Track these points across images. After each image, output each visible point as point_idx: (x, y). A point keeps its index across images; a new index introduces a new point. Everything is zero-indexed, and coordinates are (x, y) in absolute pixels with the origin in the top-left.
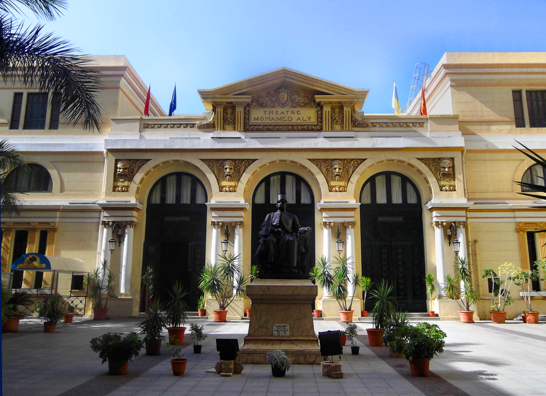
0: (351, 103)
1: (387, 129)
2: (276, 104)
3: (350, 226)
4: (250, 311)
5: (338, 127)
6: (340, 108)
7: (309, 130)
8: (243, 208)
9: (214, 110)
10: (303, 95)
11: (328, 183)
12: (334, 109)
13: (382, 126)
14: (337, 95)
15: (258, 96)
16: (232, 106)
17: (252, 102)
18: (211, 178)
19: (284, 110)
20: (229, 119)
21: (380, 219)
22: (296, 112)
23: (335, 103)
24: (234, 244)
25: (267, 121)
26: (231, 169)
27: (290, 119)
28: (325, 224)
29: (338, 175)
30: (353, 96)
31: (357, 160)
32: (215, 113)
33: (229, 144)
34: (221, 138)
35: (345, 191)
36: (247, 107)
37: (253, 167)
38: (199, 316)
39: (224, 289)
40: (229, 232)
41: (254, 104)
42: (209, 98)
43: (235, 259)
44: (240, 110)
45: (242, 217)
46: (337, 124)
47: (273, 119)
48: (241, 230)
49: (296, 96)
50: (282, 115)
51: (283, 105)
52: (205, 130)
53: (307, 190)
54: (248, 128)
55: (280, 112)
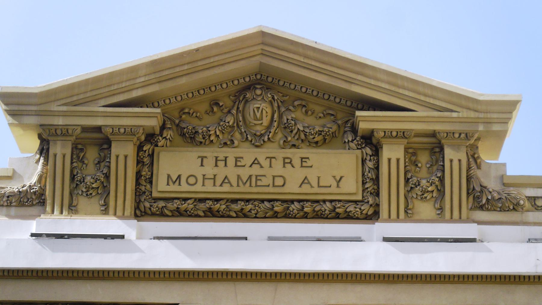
5: (426, 208)
6: (432, 152)
7: (336, 216)
9: (44, 150)
10: (318, 109)
12: (414, 154)
14: (422, 113)
15: (183, 109)
16: (101, 140)
17: (163, 127)
19: (261, 154)
20: (88, 179)
22: (297, 162)
23: (418, 135)
30: (472, 114)
32: (47, 160)
41: (168, 134)
42: (28, 114)
44: (123, 151)
49: (298, 114)
50: (256, 170)
51: (258, 140)
52: (13, 211)
54: (147, 207)
55: (248, 160)
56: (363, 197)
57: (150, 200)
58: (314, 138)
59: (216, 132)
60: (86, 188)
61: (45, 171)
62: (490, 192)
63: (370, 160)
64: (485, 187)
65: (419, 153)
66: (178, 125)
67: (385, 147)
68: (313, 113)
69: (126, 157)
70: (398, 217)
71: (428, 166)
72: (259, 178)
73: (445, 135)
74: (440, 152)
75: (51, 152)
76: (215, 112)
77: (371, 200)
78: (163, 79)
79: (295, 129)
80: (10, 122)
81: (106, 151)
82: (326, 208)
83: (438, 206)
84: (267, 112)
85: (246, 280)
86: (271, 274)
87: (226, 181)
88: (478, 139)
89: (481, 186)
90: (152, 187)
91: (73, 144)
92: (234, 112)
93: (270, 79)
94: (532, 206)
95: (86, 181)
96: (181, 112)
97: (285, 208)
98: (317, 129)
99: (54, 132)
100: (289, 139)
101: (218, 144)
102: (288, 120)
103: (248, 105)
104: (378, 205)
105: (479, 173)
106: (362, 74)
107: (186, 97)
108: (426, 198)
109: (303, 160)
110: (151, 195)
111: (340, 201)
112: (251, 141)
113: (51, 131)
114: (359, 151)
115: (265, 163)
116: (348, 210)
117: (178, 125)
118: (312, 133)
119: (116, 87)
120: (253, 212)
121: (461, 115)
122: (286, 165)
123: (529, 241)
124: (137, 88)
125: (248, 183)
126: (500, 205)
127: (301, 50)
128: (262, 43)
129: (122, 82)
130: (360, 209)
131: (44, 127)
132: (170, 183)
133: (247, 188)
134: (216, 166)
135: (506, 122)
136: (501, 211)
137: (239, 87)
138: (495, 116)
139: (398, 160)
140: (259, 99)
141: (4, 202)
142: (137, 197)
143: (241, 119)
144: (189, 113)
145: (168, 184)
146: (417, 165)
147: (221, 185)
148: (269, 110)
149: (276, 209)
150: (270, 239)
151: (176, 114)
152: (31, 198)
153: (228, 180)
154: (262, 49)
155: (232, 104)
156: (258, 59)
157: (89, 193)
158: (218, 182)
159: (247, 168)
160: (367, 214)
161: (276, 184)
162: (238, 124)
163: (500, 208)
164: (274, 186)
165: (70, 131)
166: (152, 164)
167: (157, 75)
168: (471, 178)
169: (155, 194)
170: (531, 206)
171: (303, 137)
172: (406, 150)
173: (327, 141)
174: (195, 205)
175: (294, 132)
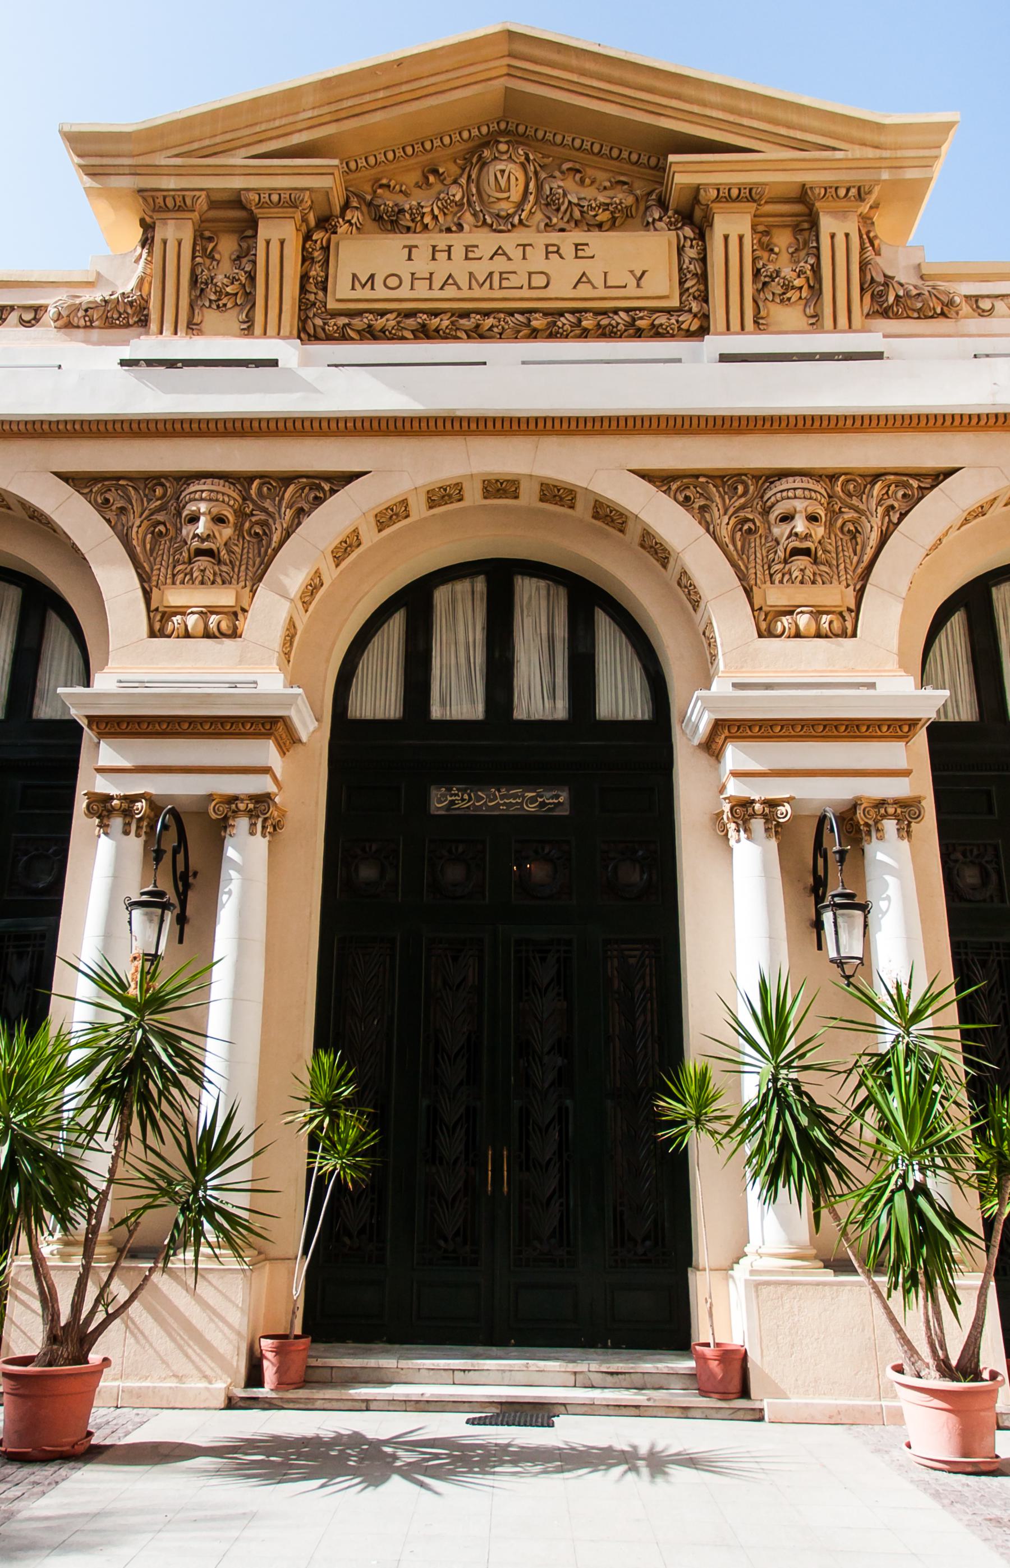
0: (860, 197)
5: (791, 315)
6: (797, 229)
8: (273, 721)
11: (748, 592)
15: (378, 184)
17: (346, 206)
19: (509, 241)
20: (220, 279)
22: (568, 250)
25: (422, 290)
26: (219, 520)
29: (806, 552)
30: (870, 153)
31: (902, 476)
32: (150, 253)
34: (171, 364)
35: (844, 634)
42: (115, 171)
44: (279, 235)
45: (266, 770)
46: (785, 301)
48: (260, 844)
49: (569, 184)
50: (500, 264)
51: (504, 223)
52: (95, 334)
54: (317, 323)
56: (681, 303)
57: (324, 316)
58: (596, 215)
59: (432, 210)
60: (215, 293)
62: (902, 285)
63: (692, 247)
64: (893, 278)
65: (775, 232)
66: (370, 204)
67: (718, 220)
68: (593, 183)
69: (282, 243)
70: (743, 328)
71: (791, 250)
72: (504, 276)
73: (823, 191)
74: (810, 229)
76: (431, 184)
77: (695, 307)
78: (343, 114)
79: (563, 202)
80: (88, 185)
81: (250, 241)
82: (620, 321)
83: (810, 311)
84: (517, 179)
87: (450, 281)
88: (875, 207)
89: (885, 276)
90: (326, 296)
91: (195, 231)
92: (463, 181)
94: (974, 310)
95: (215, 281)
96: (376, 185)
97: (548, 323)
98: (602, 199)
99: (162, 204)
100: (555, 220)
101: (437, 229)
102: (551, 189)
103: (485, 170)
104: (706, 317)
106: (679, 97)
107: (384, 159)
108: (789, 299)
109: (579, 247)
110: (325, 307)
111: (640, 309)
112: (492, 225)
113: (157, 201)
115: (516, 254)
116: (656, 322)
117: (370, 204)
118: (594, 205)
119: (263, 127)
120: (495, 330)
121: (850, 155)
122: (550, 255)
123: (975, 356)
124: (301, 131)
126: (919, 305)
127: (574, 62)
128: (509, 56)
129: (274, 119)
130: (677, 321)
131: (145, 194)
132: (357, 284)
133: (485, 292)
134: (434, 259)
135: (928, 163)
136: (919, 318)
137: (470, 144)
139: (741, 238)
140: (505, 157)
141: (79, 319)
142: (302, 313)
143: (474, 191)
144: (389, 186)
145: (353, 288)
146: (772, 250)
147: (441, 288)
148: (520, 175)
149: (534, 323)
150: (523, 363)
151: (368, 188)
152: (125, 312)
153: (453, 279)
154: (509, 66)
155: (459, 171)
157: (221, 303)
158: (437, 284)
159: (485, 260)
160: (688, 330)
161: (533, 285)
162: (468, 200)
163: (919, 311)
164: (530, 287)
165: (189, 202)
166: (327, 261)
167: (333, 107)
168: (868, 263)
169: (331, 305)
170: (970, 310)
171: (577, 214)
173: (617, 224)
174: (399, 323)
175: (563, 208)
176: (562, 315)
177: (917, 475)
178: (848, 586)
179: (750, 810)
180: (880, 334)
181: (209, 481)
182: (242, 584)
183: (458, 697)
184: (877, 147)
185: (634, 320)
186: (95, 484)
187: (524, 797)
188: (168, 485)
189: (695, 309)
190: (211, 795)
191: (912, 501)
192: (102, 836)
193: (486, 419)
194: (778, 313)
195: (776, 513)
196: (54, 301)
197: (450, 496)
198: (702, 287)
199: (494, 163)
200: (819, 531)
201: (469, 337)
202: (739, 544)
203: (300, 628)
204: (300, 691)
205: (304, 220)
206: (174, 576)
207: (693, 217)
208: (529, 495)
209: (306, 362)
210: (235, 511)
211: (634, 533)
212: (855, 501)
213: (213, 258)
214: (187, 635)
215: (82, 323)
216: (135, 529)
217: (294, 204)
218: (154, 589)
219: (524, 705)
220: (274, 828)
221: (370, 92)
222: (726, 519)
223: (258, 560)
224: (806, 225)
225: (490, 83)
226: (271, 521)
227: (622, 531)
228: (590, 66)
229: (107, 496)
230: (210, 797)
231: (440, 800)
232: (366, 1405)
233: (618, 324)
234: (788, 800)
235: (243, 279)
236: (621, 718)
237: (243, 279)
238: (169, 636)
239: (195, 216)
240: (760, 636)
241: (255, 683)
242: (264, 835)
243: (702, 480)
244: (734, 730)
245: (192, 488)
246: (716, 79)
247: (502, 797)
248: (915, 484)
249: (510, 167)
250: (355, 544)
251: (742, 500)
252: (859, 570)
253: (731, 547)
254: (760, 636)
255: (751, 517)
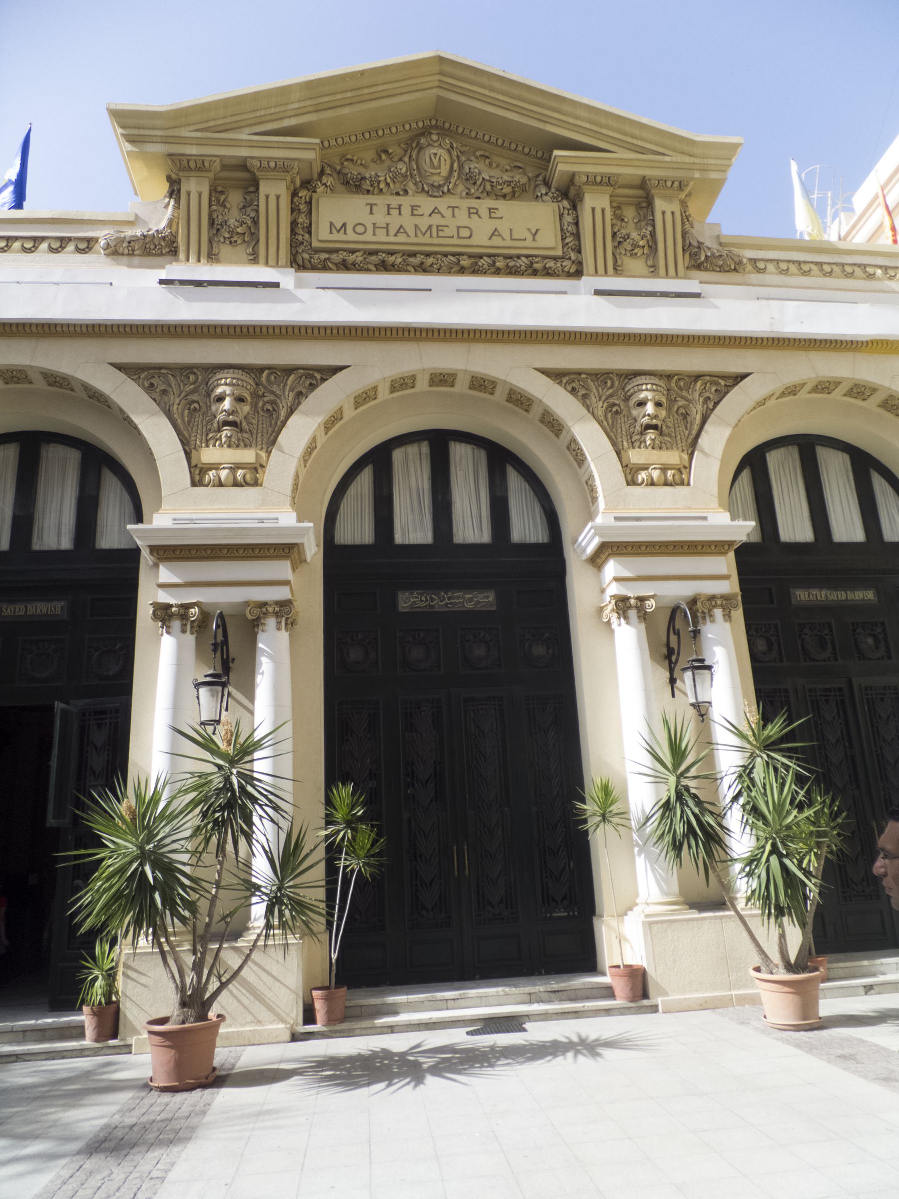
0: (681, 188)
1: (804, 280)
2: (411, 187)
3: (718, 613)
4: (327, 999)
5: (637, 265)
6: (638, 207)
11: (618, 454)
13: (785, 272)
15: (344, 158)
17: (322, 173)
18: (159, 433)
19: (442, 204)
20: (232, 222)
21: (802, 595)
22: (484, 212)
24: (251, 697)
25: (381, 236)
26: (240, 400)
27: (465, 233)
28: (622, 605)
29: (655, 427)
30: (687, 159)
32: (178, 201)
33: (232, 305)
34: (199, 284)
35: (682, 483)
36: (304, 189)
37: (330, 395)
38: (88, 1042)
39: (203, 905)
40: (233, 651)
42: (152, 140)
43: (257, 745)
44: (274, 192)
45: (287, 583)
46: (633, 255)
47: (400, 230)
48: (284, 635)
50: (436, 220)
51: (436, 191)
52: (136, 260)
53: (531, 494)
54: (305, 256)
61: (176, 214)
62: (709, 249)
63: (568, 214)
64: (703, 243)
65: (623, 207)
66: (339, 173)
69: (278, 197)
71: (636, 221)
72: (440, 228)
73: (657, 182)
75: (184, 189)
78: (321, 107)
81: (253, 195)
83: (650, 263)
85: (433, 340)
86: (463, 331)
87: (402, 230)
88: (689, 195)
91: (210, 186)
92: (406, 159)
93: (447, 125)
98: (506, 178)
100: (473, 191)
103: (422, 152)
105: (693, 231)
108: (636, 254)
110: (310, 245)
111: (536, 256)
114: (556, 204)
115: (448, 213)
116: (547, 266)
117: (339, 173)
119: (262, 113)
120: (435, 266)
121: (674, 159)
124: (290, 117)
125: (429, 232)
126: (721, 263)
127: (486, 81)
128: (441, 73)
129: (270, 107)
132: (334, 230)
133: (426, 239)
134: (389, 214)
135: (724, 169)
138: (713, 161)
139: (603, 210)
140: (436, 144)
143: (415, 167)
144: (352, 160)
145: (331, 232)
146: (623, 220)
147: (395, 235)
148: (447, 157)
149: (462, 263)
151: (337, 160)
154: (439, 81)
155: (403, 152)
156: (436, 92)
157: (233, 240)
158: (392, 232)
159: (426, 217)
161: (461, 235)
163: (720, 267)
164: (459, 237)
165: (206, 164)
166: (310, 212)
167: (314, 102)
169: (315, 244)
171: (488, 187)
172: (611, 202)
174: (365, 259)
176: (481, 257)
177: (724, 377)
178: (683, 451)
179: (628, 604)
180: (697, 281)
181: (231, 371)
182: (259, 447)
183: (413, 527)
184: (691, 156)
185: (532, 263)
186: (142, 372)
187: (464, 598)
188: (199, 373)
189: (573, 258)
190: (247, 602)
191: (722, 394)
192: (165, 634)
193: (433, 330)
194: (629, 263)
195: (634, 400)
196: (103, 234)
197: (406, 384)
198: (577, 243)
199: (430, 148)
200: (663, 413)
201: (416, 271)
202: (610, 421)
203: (301, 478)
204: (311, 525)
205: (293, 181)
206: (207, 441)
207: (569, 194)
208: (461, 385)
209: (299, 285)
210: (251, 394)
211: (536, 411)
212: (684, 393)
213: (225, 206)
214: (221, 485)
215: (126, 251)
216: (175, 406)
217: (286, 169)
218: (194, 452)
219: (461, 533)
220: (291, 624)
221: (341, 92)
222: (601, 404)
223: (270, 430)
224: (645, 204)
225: (427, 91)
226: (278, 401)
227: (527, 411)
228: (497, 85)
229: (153, 381)
230: (247, 603)
231: (408, 601)
232: (392, 1029)
233: (521, 266)
234: (653, 597)
235: (249, 222)
236: (528, 542)
237: (249, 222)
238: (207, 486)
239: (211, 175)
240: (628, 484)
241: (277, 519)
242: (286, 630)
243: (583, 376)
244: (615, 549)
245: (218, 376)
246: (585, 100)
247: (449, 598)
248: (723, 383)
249: (441, 152)
250: (339, 417)
251: (611, 391)
252: (690, 440)
253: (605, 423)
254: (628, 484)
255: (617, 402)
